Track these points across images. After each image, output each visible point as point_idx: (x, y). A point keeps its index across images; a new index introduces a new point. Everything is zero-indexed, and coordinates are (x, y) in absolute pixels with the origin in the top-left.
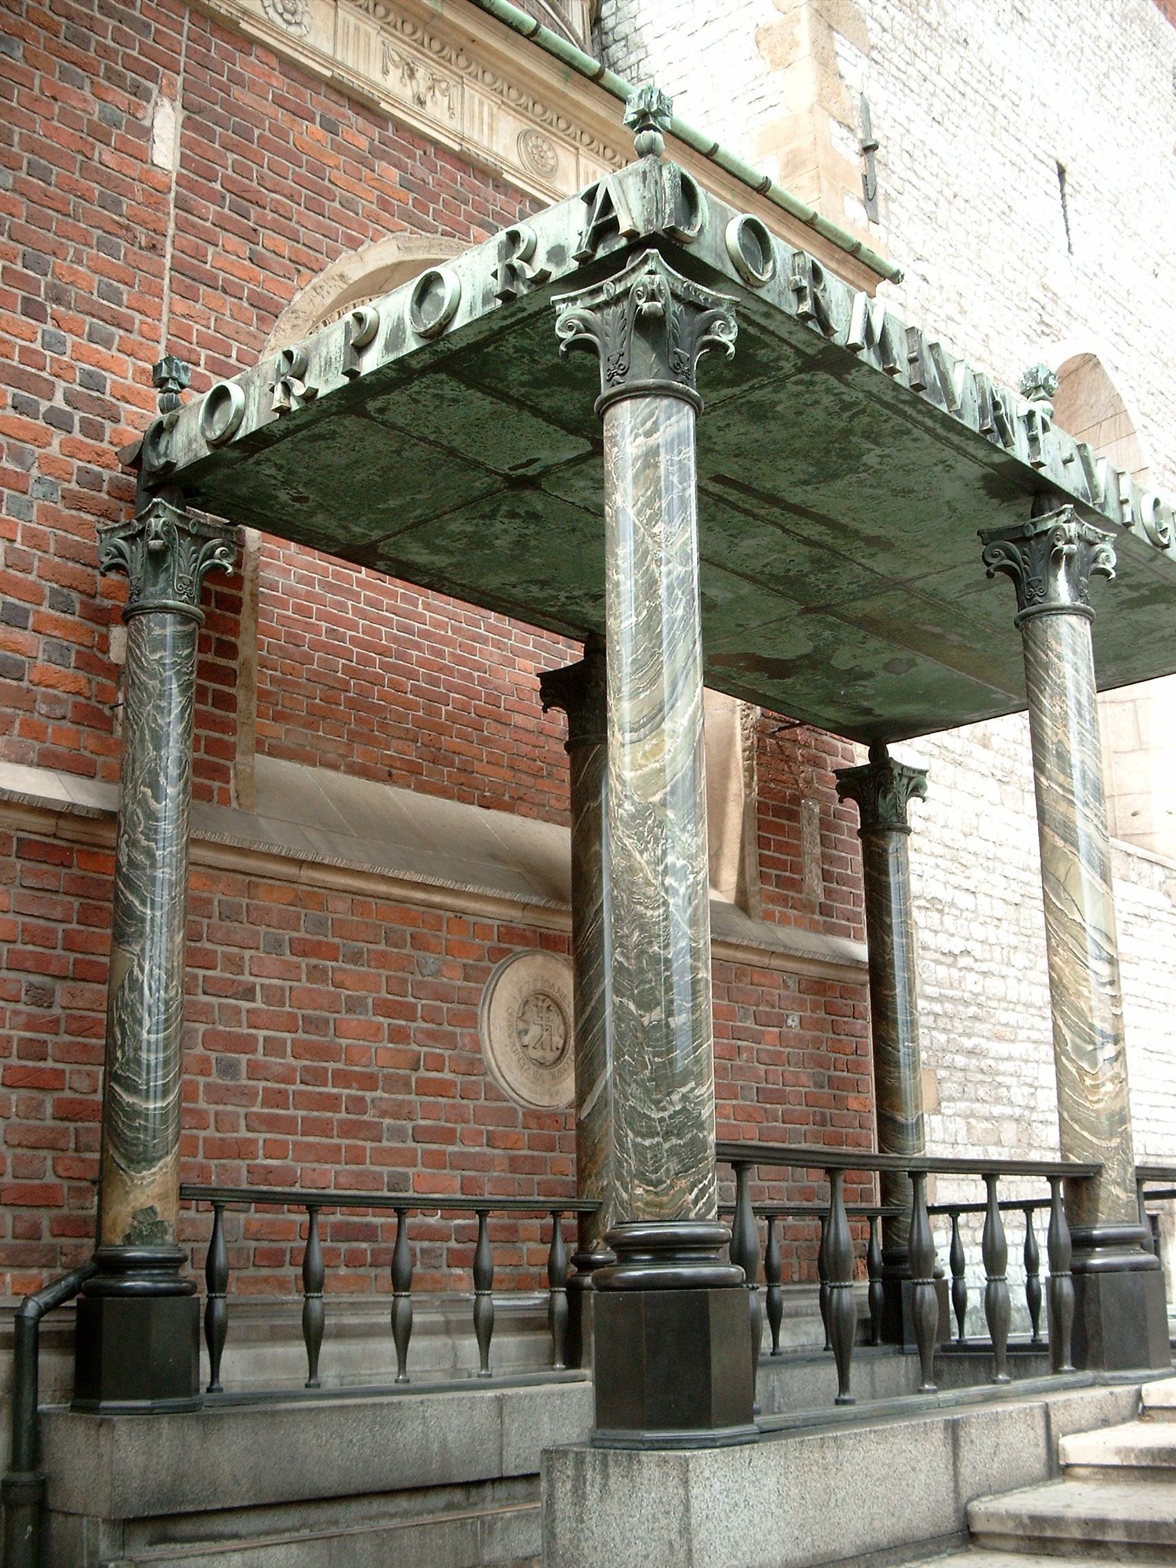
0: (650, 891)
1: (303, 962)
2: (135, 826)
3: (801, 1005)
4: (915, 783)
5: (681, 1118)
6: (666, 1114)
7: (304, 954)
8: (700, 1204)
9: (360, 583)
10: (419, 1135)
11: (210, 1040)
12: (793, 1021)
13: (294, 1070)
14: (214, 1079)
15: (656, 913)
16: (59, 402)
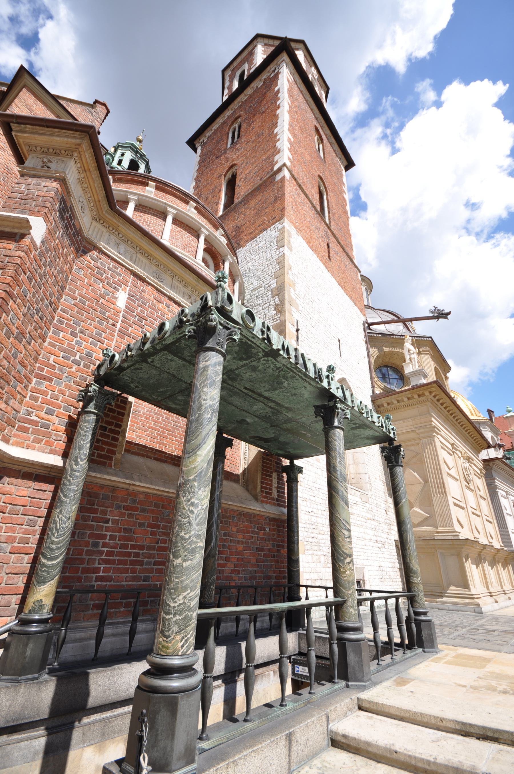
0: (184, 512)
1: (127, 512)
2: (67, 473)
3: (270, 525)
4: (300, 470)
5: (182, 606)
6: (176, 605)
7: (128, 510)
8: (185, 647)
9: (164, 413)
10: (156, 563)
11: (91, 536)
12: (267, 529)
13: (118, 544)
14: (90, 548)
15: (185, 520)
16: (77, 358)
